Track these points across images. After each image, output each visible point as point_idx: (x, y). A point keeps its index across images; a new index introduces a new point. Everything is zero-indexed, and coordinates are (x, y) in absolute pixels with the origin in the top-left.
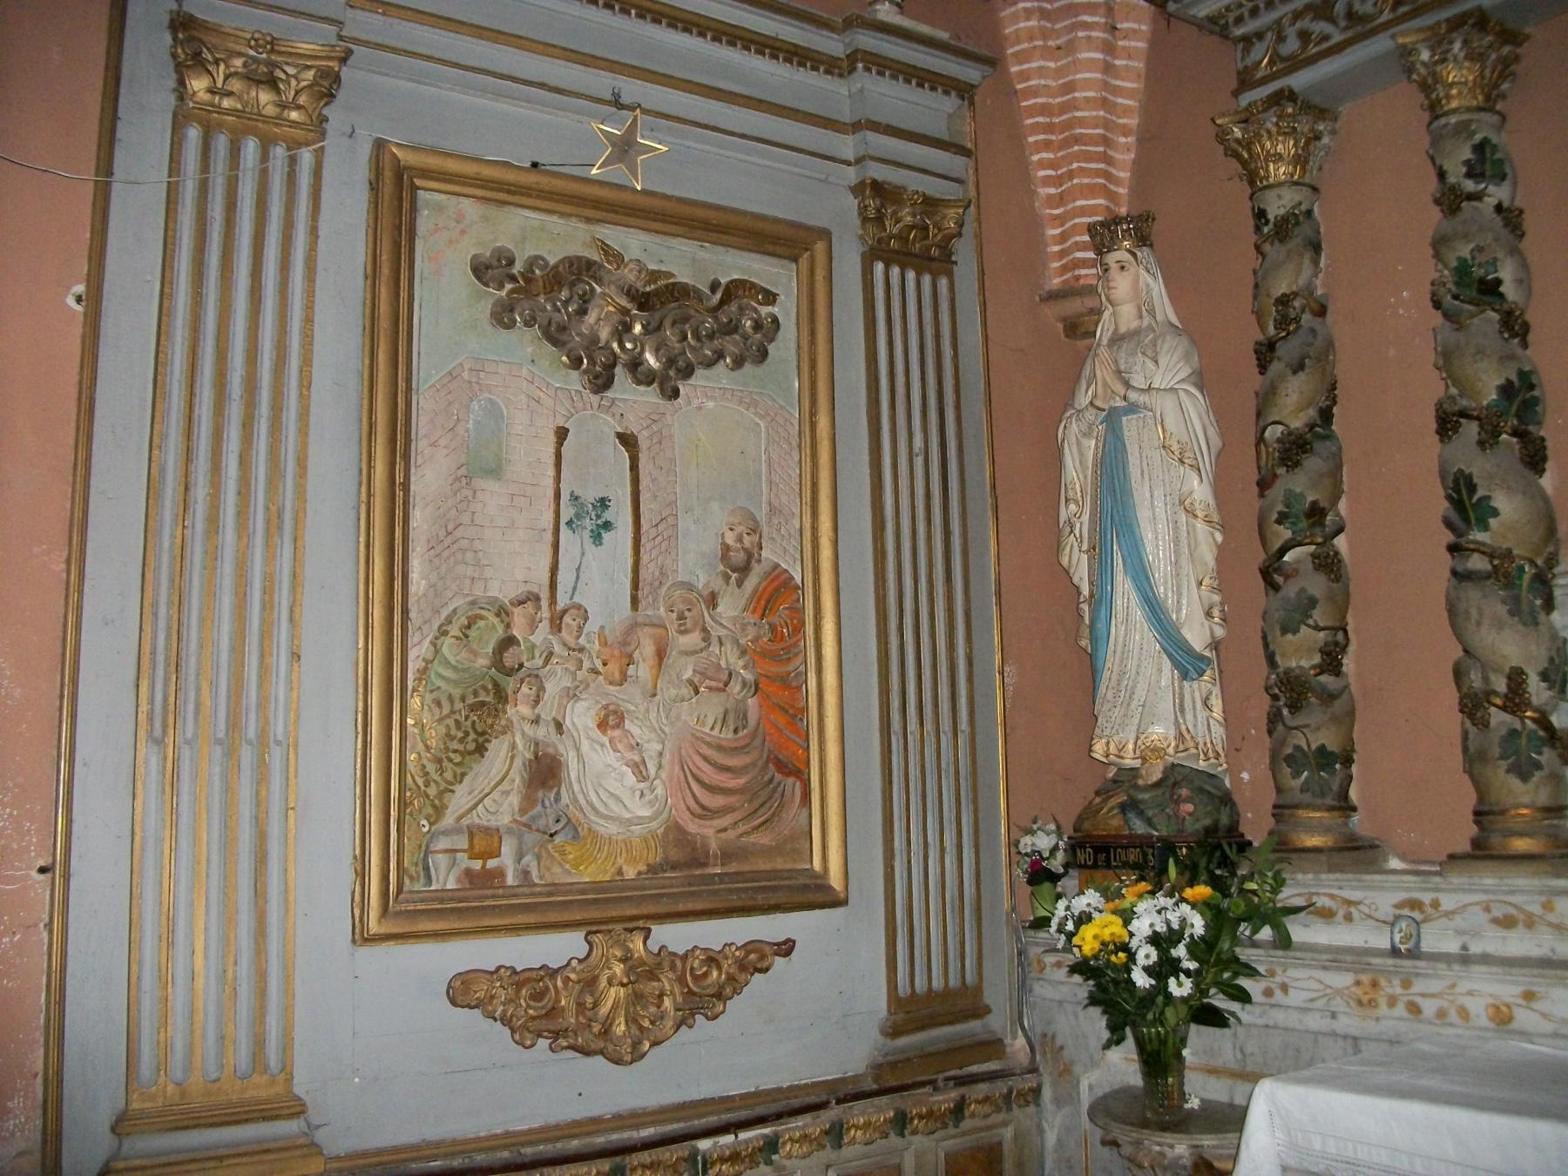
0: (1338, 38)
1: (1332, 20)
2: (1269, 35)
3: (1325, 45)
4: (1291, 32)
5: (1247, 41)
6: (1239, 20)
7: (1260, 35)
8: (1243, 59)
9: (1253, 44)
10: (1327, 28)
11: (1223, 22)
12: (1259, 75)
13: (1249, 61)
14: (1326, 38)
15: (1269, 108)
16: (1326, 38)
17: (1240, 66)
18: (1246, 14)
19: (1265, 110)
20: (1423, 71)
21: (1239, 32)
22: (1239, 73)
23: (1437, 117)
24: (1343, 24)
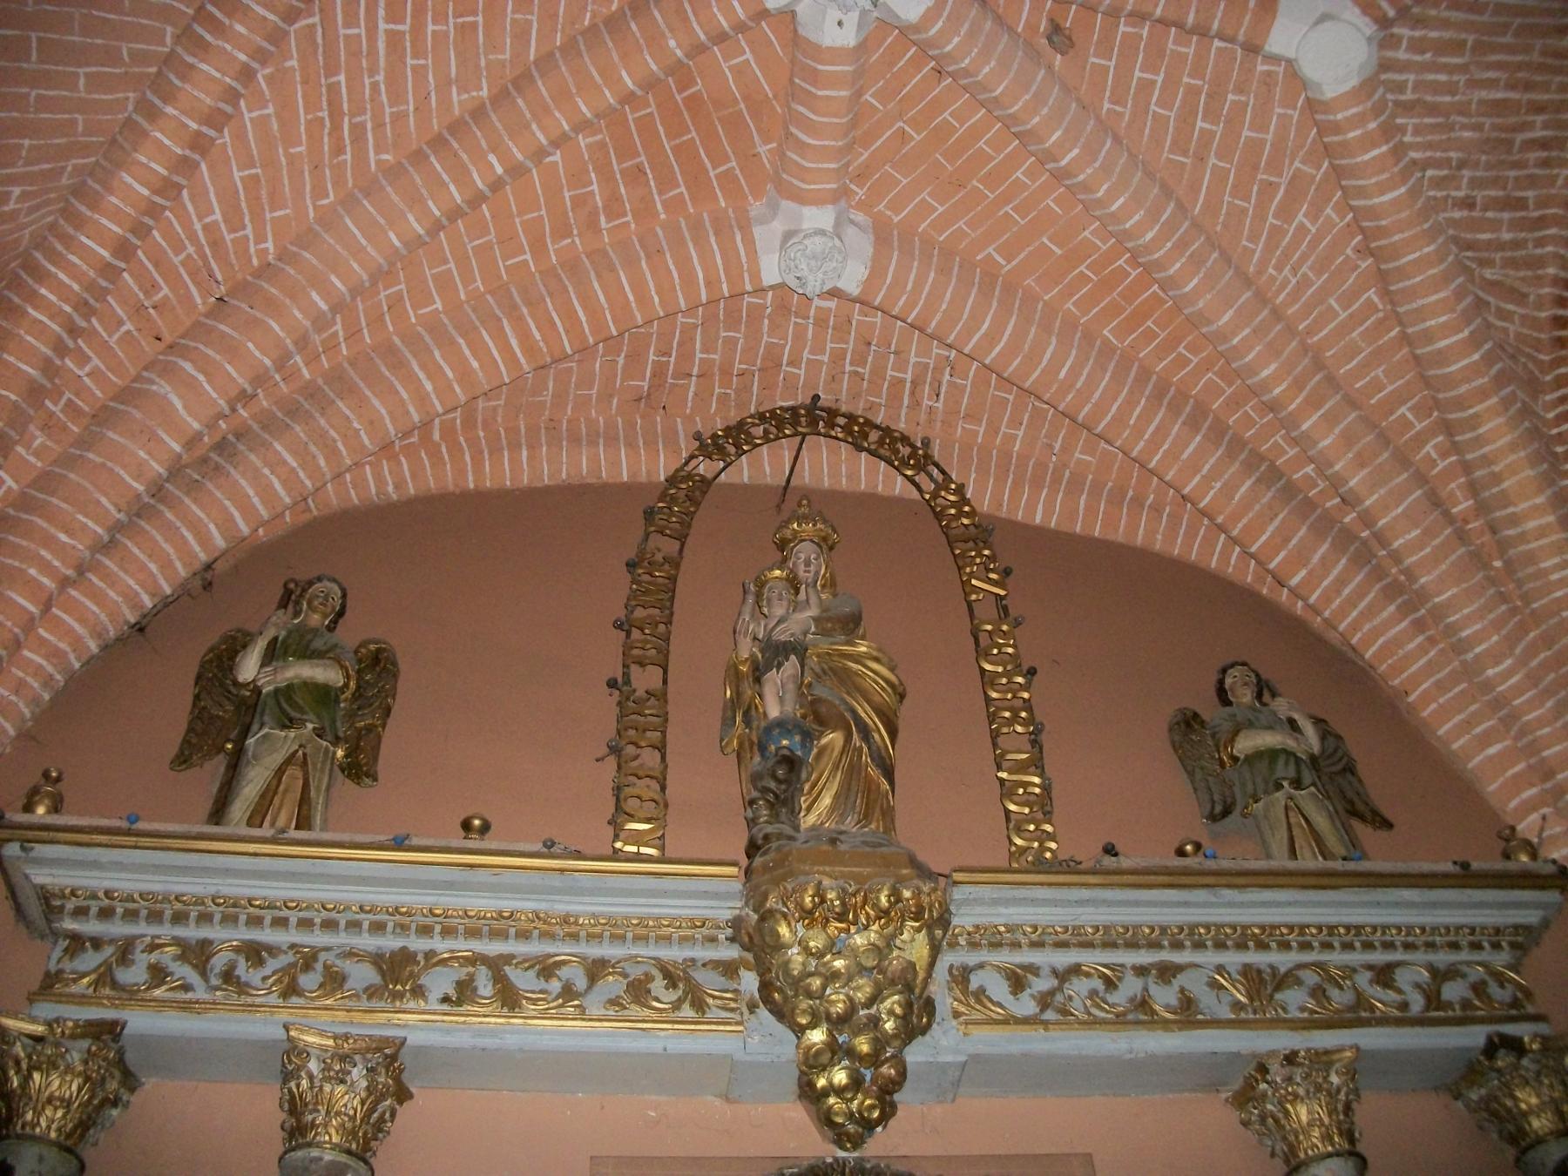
0: (201, 993)
1: (204, 974)
2: (109, 951)
3: (181, 996)
4: (142, 959)
5: (77, 943)
6: (81, 912)
7: (97, 943)
8: (58, 962)
9: (83, 949)
10: (193, 977)
11: (58, 903)
12: (74, 989)
13: (67, 965)
14: (186, 988)
15: (83, 1036)
16: (186, 988)
17: (53, 967)
18: (94, 910)
19: (73, 1037)
20: (305, 1083)
21: (69, 925)
22: (47, 974)
23: (299, 1147)
24: (215, 981)
